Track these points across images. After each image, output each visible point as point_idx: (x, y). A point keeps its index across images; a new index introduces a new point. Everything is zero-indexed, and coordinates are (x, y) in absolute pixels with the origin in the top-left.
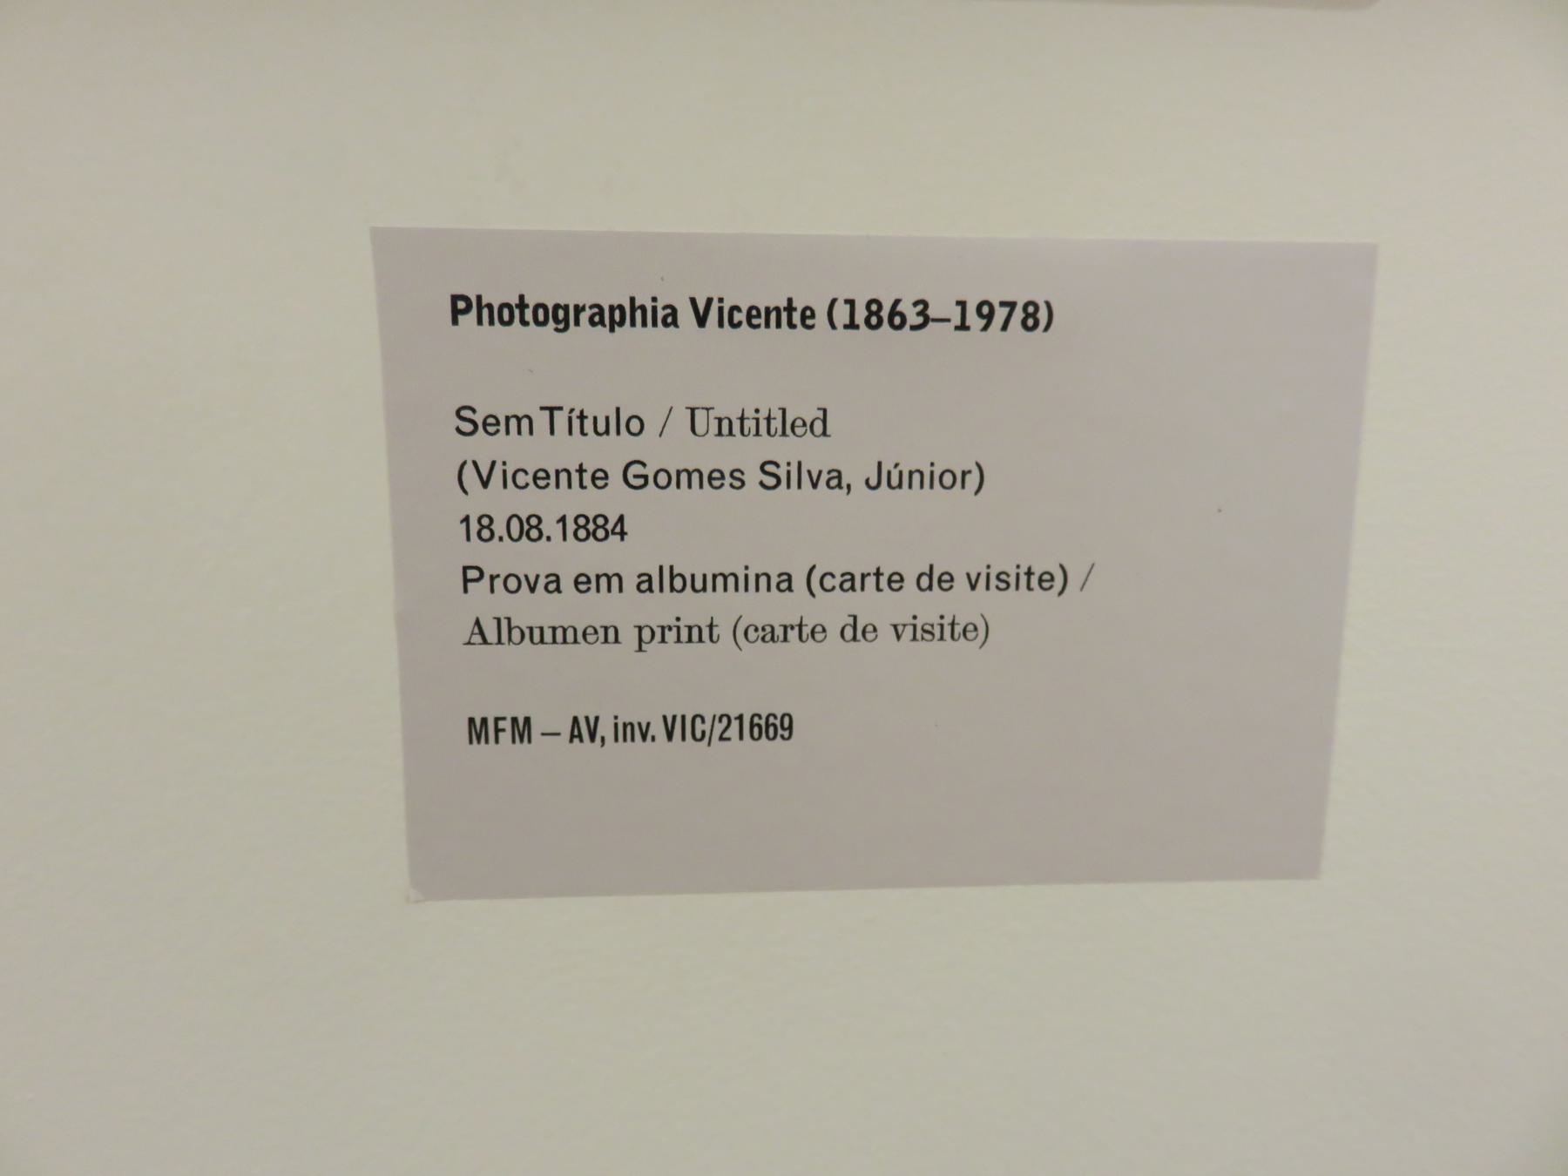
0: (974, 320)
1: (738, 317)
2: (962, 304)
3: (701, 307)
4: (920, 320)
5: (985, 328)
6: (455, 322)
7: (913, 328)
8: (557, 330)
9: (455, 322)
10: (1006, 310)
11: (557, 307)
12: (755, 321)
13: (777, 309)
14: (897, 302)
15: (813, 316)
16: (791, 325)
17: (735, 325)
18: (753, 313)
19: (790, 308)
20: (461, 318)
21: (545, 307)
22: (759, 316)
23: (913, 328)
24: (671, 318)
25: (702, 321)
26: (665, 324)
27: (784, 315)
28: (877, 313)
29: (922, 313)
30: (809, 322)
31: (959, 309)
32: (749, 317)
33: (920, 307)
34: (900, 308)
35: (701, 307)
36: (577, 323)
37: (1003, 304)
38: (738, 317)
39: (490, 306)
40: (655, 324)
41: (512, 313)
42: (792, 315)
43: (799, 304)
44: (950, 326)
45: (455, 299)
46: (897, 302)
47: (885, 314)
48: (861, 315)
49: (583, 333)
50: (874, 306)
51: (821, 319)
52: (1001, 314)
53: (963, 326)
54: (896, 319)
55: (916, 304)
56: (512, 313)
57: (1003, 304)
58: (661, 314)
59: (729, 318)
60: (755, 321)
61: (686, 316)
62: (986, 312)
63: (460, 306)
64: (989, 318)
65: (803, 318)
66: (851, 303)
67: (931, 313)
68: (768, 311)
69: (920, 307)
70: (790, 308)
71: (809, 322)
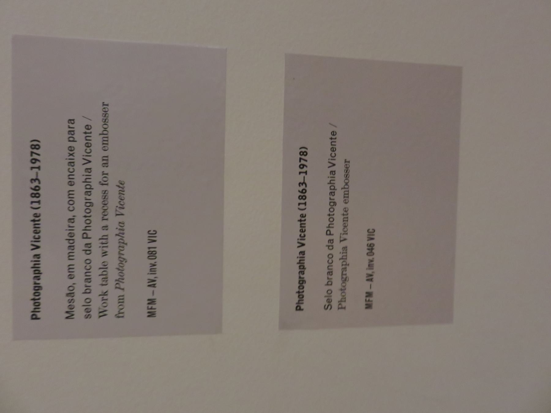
0: (304, 170)
1: (302, 235)
2: (300, 173)
3: (300, 245)
4: (304, 185)
5: (307, 167)
6: (302, 310)
7: (306, 186)
8: (305, 283)
9: (302, 310)
10: (302, 161)
11: (299, 283)
12: (304, 230)
13: (301, 224)
14: (299, 191)
15: (303, 214)
16: (305, 220)
17: (305, 236)
18: (302, 231)
19: (300, 221)
20: (302, 308)
21: (299, 287)
22: (302, 230)
23: (306, 186)
24: (302, 253)
25: (303, 245)
26: (304, 254)
27: (302, 222)
28: (302, 197)
29: (302, 184)
30: (304, 215)
31: (301, 174)
32: (302, 232)
33: (301, 185)
34: (301, 190)
35: (300, 245)
36: (303, 278)
37: (300, 161)
38: (302, 235)
39: (299, 301)
40: (304, 257)
41: (301, 295)
42: (302, 220)
43: (299, 218)
44: (306, 176)
45: (297, 309)
46: (299, 191)
47: (302, 195)
48: (302, 201)
49: (306, 276)
50: (300, 198)
51: (303, 212)
52: (303, 162)
53: (306, 173)
54: (304, 191)
55: (300, 186)
56: (301, 295)
57: (300, 161)
58: (301, 256)
59: (303, 237)
60: (304, 230)
61: (302, 249)
62: (302, 166)
63: (299, 308)
64: (304, 165)
65: (303, 217)
66: (299, 204)
67: (302, 181)
68: (301, 227)
69: (301, 185)
70: (300, 221)
71: (304, 215)
